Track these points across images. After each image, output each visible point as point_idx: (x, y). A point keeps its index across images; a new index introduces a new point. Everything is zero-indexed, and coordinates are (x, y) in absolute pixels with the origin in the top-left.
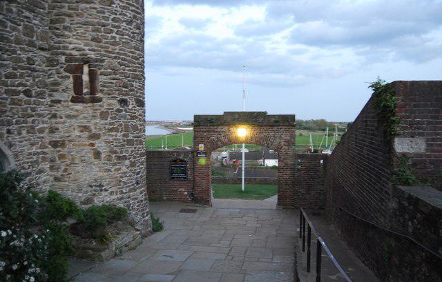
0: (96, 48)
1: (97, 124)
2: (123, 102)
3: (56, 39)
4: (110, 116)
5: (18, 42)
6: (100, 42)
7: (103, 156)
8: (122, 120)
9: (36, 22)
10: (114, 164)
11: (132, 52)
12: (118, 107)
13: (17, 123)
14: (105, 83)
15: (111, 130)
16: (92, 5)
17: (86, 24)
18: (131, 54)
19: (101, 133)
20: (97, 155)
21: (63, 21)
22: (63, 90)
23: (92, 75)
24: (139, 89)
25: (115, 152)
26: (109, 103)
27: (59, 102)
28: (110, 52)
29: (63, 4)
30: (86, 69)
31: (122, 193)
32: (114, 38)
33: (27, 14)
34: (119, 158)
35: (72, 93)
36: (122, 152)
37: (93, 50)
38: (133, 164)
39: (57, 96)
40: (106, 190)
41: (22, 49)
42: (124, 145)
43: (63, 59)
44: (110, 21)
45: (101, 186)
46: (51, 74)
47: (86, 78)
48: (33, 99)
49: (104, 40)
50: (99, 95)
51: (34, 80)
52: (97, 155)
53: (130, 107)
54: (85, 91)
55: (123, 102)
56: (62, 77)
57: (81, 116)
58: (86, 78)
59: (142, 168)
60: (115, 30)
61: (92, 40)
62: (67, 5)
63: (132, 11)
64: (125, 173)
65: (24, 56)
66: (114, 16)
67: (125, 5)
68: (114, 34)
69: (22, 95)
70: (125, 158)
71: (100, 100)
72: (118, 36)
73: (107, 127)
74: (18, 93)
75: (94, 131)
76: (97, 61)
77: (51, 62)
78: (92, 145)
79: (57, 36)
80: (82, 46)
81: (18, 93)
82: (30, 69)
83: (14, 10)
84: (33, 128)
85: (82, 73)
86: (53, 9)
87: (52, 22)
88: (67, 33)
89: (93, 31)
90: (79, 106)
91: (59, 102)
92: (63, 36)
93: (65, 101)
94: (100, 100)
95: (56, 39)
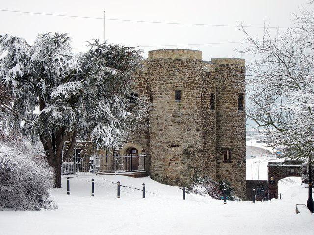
1: (231, 170)
2: (239, 162)
8: (239, 168)
15: (235, 172)
23: (229, 153)
26: (235, 162)
30: (228, 152)
34: (238, 181)
35: (223, 160)
38: (242, 184)
39: (219, 161)
43: (221, 149)
47: (228, 155)
50: (232, 160)
58: (228, 155)
71: (232, 162)
81: (210, 161)
90: (226, 164)
91: (219, 163)
94: (232, 162)
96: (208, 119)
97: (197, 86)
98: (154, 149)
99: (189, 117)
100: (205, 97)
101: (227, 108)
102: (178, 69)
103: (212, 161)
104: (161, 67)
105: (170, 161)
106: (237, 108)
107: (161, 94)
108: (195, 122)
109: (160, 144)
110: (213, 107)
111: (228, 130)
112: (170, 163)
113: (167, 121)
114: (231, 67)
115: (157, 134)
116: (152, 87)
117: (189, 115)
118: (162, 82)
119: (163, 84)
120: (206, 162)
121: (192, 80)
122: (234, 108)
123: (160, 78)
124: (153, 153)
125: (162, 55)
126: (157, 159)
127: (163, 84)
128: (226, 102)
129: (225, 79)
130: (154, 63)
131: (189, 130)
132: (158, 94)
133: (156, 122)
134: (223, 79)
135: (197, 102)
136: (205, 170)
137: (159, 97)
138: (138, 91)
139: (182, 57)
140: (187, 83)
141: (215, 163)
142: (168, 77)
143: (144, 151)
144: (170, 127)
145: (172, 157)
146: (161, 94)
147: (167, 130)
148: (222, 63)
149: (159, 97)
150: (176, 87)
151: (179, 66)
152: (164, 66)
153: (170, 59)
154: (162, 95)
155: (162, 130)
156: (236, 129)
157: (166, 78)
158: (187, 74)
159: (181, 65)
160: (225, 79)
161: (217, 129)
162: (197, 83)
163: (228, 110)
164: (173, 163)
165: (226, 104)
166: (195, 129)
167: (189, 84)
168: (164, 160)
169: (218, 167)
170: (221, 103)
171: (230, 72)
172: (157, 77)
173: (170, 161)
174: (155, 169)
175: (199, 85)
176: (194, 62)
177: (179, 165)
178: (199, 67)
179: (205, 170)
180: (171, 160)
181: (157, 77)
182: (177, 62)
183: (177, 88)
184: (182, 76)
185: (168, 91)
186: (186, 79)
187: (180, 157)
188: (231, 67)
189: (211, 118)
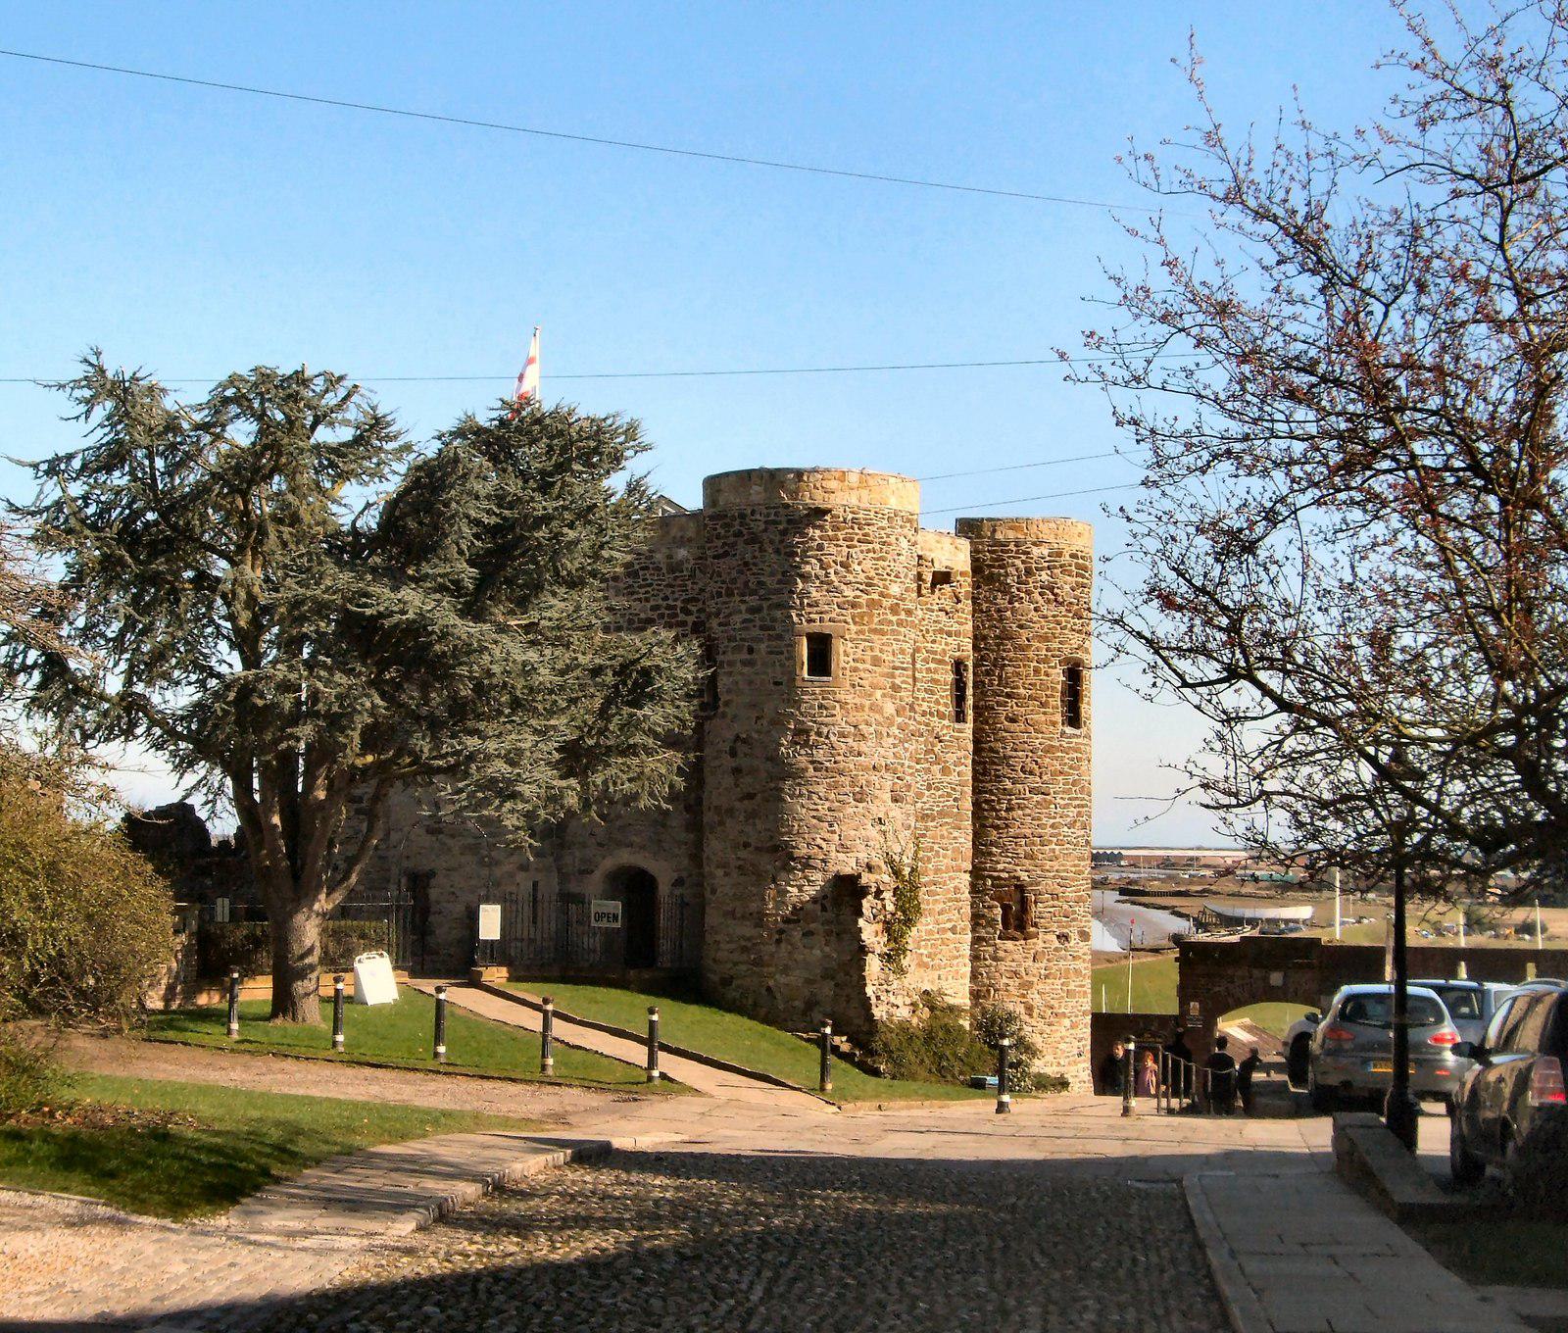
2: (1063, 937)
8: (1062, 962)
12: (1057, 944)
15: (1046, 977)
16: (1028, 811)
19: (1035, 980)
20: (1029, 1009)
32: (1053, 850)
33: (956, 834)
35: (1000, 927)
38: (1074, 1026)
39: (983, 933)
49: (1040, 856)
52: (1029, 1009)
55: (1063, 937)
59: (1086, 1032)
69: (950, 934)
74: (944, 930)
77: (974, 889)
78: (1023, 996)
81: (944, 930)
84: (957, 972)
90: (1009, 944)
92: (991, 854)
94: (1036, 935)
97: (894, 619)
98: (720, 872)
99: (863, 748)
100: (929, 670)
103: (953, 930)
104: (754, 539)
106: (1058, 718)
109: (743, 854)
110: (960, 717)
112: (781, 932)
114: (1036, 551)
115: (730, 811)
116: (714, 623)
118: (752, 601)
119: (759, 610)
121: (875, 596)
123: (746, 584)
124: (714, 891)
125: (757, 493)
126: (732, 914)
128: (1008, 696)
130: (727, 526)
132: (737, 649)
133: (728, 762)
136: (926, 966)
137: (745, 663)
140: (854, 606)
141: (969, 937)
142: (780, 582)
143: (679, 883)
146: (751, 651)
149: (745, 663)
150: (810, 621)
151: (821, 538)
154: (755, 656)
155: (750, 796)
157: (771, 582)
159: (830, 533)
161: (976, 804)
162: (894, 609)
166: (887, 796)
169: (975, 958)
170: (992, 701)
171: (1029, 572)
172: (734, 581)
174: (720, 955)
175: (903, 616)
176: (884, 523)
177: (819, 939)
178: (904, 543)
179: (926, 966)
181: (734, 581)
183: (815, 628)
184: (833, 577)
188: (1036, 551)
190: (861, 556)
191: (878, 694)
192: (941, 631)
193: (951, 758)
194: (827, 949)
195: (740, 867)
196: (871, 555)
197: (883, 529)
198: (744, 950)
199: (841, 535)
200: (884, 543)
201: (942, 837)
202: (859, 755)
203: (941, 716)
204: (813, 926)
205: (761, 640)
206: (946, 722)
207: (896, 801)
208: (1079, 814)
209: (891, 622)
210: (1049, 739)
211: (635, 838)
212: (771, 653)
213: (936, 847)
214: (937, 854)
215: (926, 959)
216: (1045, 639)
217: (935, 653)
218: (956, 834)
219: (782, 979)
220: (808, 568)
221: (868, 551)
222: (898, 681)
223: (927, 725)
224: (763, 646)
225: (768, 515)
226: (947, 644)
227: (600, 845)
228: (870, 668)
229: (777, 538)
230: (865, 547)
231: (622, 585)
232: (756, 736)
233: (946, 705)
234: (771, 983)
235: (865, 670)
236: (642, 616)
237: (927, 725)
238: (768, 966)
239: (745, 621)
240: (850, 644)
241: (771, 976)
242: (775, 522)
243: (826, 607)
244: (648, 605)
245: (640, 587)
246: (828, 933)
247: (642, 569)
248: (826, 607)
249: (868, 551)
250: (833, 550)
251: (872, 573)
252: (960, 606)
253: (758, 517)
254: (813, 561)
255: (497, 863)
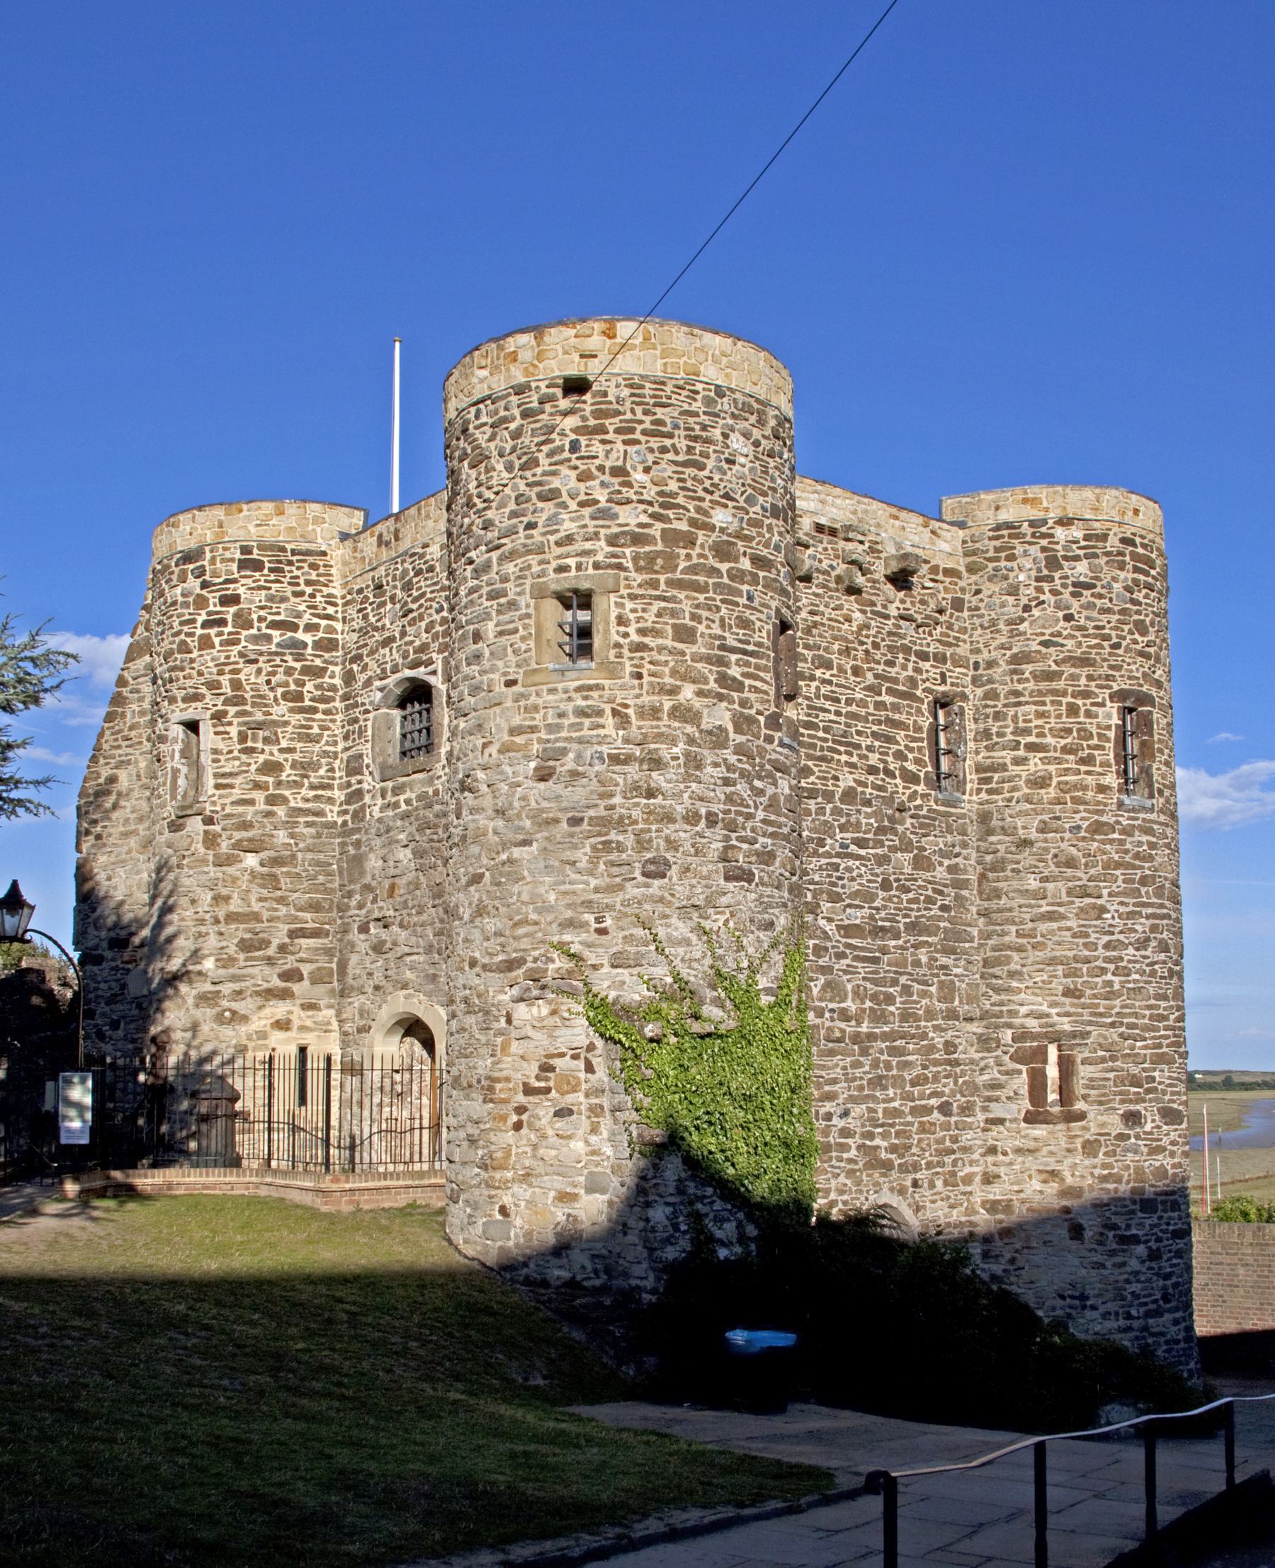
0: (1073, 1010)
2: (1132, 1118)
3: (995, 998)
4: (1103, 1150)
5: (930, 1015)
6: (1079, 997)
7: (1088, 1234)
9: (959, 971)
10: (1113, 1253)
11: (1150, 1007)
13: (929, 1165)
14: (1091, 1080)
16: (1064, 923)
17: (1052, 961)
18: (1147, 1012)
21: (1008, 960)
22: (1009, 1098)
23: (1066, 1066)
24: (1170, 1085)
25: (1114, 1227)
27: (1001, 1121)
28: (1101, 1015)
29: (1006, 927)
30: (1053, 1053)
31: (1129, 1316)
32: (1110, 984)
33: (944, 960)
34: (1123, 1240)
35: (1026, 1104)
36: (1128, 1227)
37: (1067, 1014)
38: (1154, 1255)
39: (997, 1111)
40: (1094, 1308)
41: (936, 1028)
42: (1133, 1212)
43: (1007, 1035)
44: (1101, 950)
45: (1083, 1297)
46: (986, 1067)
47: (1052, 1072)
48: (953, 1119)
49: (1088, 992)
50: (1080, 1106)
51: (956, 1083)
53: (1148, 1127)
54: (1052, 1097)
55: (1132, 1118)
56: (1007, 1073)
57: (1045, 1151)
60: (1112, 967)
61: (1064, 995)
62: (1013, 929)
63: (1148, 917)
64: (1136, 1273)
65: (939, 1041)
66: (1106, 938)
67: (1131, 908)
68: (1109, 977)
70: (1135, 1240)
71: (1082, 1116)
72: (1116, 979)
73: (1097, 1172)
74: (928, 1110)
75: (1069, 1180)
76: (1075, 1037)
77: (985, 1043)
79: (997, 990)
80: (1044, 1008)
81: (928, 1110)
82: (949, 1062)
83: (924, 959)
84: (953, 1174)
85: (1045, 1061)
86: (989, 937)
87: (986, 963)
88: (1015, 984)
89: (1065, 976)
90: (1040, 1131)
91: (1001, 1121)
92: (1008, 990)
93: (1015, 1120)
95: (995, 998)
96: (906, 846)
97: (724, 567)
100: (879, 705)
101: (1040, 782)
102: (574, 447)
103: (945, 1109)
105: (521, 1098)
106: (1112, 780)
107: (477, 637)
108: (712, 820)
111: (1050, 917)
112: (521, 1110)
113: (500, 812)
114: (1060, 533)
117: (656, 763)
119: (487, 567)
120: (897, 1113)
121: (683, 526)
122: (1090, 780)
127: (487, 567)
128: (1031, 747)
129: (1027, 608)
131: (656, 870)
134: (1012, 611)
135: (723, 679)
138: (434, 673)
139: (591, 369)
140: (637, 539)
144: (517, 852)
145: (534, 1069)
147: (511, 872)
148: (1004, 516)
150: (562, 569)
152: (492, 445)
153: (520, 390)
155: (476, 879)
156: (1103, 910)
158: (638, 476)
159: (592, 422)
160: (1027, 608)
162: (723, 551)
163: (1052, 792)
164: (543, 1110)
165: (1035, 763)
167: (657, 552)
168: (488, 1089)
170: (1007, 756)
173: (521, 1098)
175: (745, 564)
178: (737, 442)
179: (887, 1166)
180: (528, 1090)
182: (564, 404)
184: (601, 496)
185: (513, 605)
186: (630, 517)
187: (590, 1068)
189: (933, 843)
190: (650, 458)
191: (688, 692)
192: (907, 650)
193: (933, 843)
194: (593, 1139)
195: (466, 1000)
196: (671, 456)
197: (696, 415)
198: (472, 1141)
199: (611, 424)
200: (695, 439)
201: (917, 963)
202: (651, 794)
203: (911, 778)
204: (570, 1098)
205: (488, 617)
206: (921, 788)
207: (737, 879)
208: (1154, 929)
209: (714, 572)
210: (1097, 812)
211: (409, 975)
212: (501, 633)
213: (903, 980)
214: (906, 990)
215: (883, 1155)
216: (1085, 661)
217: (896, 681)
218: (944, 960)
219: (521, 1191)
220: (555, 483)
221: (664, 450)
222: (735, 672)
223: (880, 788)
224: (491, 625)
225: (496, 412)
226: (918, 670)
227: (377, 988)
228: (669, 643)
229: (508, 447)
230: (655, 443)
231: (398, 606)
232: (480, 775)
233: (918, 761)
234: (507, 1200)
235: (661, 649)
236: (417, 643)
237: (880, 788)
238: (502, 1168)
239: (472, 591)
240: (629, 605)
241: (505, 1185)
242: (505, 420)
243: (588, 546)
244: (423, 624)
245: (416, 600)
246: (596, 1110)
247: (416, 575)
248: (588, 546)
249: (664, 450)
250: (598, 448)
251: (673, 486)
252: (942, 619)
253: (484, 419)
254: (568, 472)
255: (245, 1019)
